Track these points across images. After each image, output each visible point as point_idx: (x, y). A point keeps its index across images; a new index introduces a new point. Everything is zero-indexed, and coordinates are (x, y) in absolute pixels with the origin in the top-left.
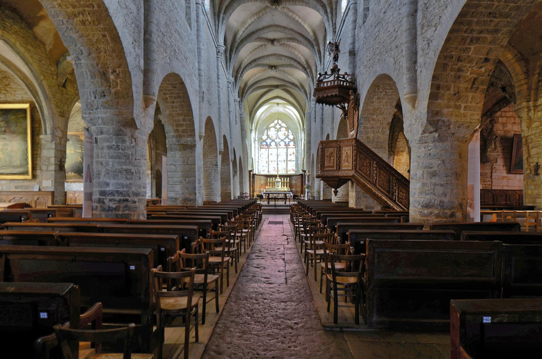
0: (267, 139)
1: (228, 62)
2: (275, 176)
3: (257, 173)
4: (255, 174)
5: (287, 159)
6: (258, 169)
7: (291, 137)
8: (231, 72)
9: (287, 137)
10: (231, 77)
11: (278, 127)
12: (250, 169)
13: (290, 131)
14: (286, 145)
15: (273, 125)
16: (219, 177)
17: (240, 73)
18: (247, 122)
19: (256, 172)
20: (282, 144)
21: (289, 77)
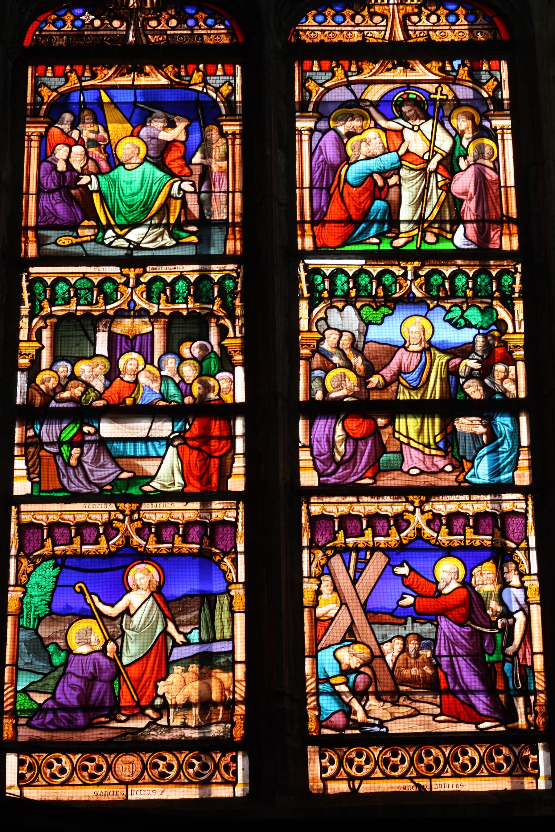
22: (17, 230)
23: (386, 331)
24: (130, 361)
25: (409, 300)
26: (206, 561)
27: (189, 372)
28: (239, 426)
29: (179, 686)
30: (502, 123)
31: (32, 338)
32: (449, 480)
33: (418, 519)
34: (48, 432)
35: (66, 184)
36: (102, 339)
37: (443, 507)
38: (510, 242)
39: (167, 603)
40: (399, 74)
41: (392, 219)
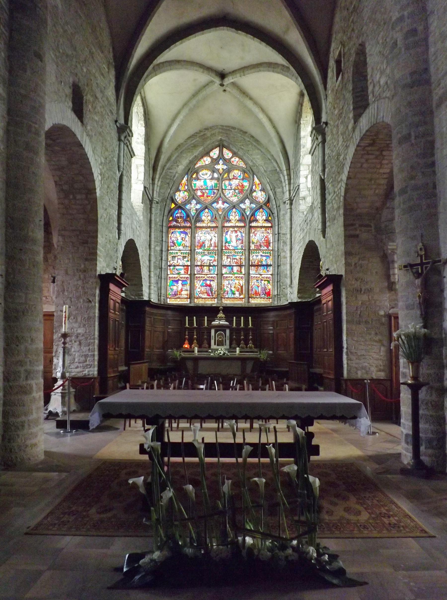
2: (212, 311)
3: (154, 299)
4: (148, 303)
6: (160, 289)
7: (260, 196)
11: (221, 166)
13: (256, 181)
15: (207, 160)
19: (149, 293)
20: (234, 216)
22: (168, 247)
23: (203, 258)
24: (179, 261)
25: (206, 255)
27: (185, 262)
28: (189, 267)
29: (183, 293)
32: (209, 273)
33: (206, 277)
34: (172, 268)
35: (173, 242)
36: (176, 258)
37: (208, 276)
38: (216, 249)
40: (206, 230)
41: (205, 246)
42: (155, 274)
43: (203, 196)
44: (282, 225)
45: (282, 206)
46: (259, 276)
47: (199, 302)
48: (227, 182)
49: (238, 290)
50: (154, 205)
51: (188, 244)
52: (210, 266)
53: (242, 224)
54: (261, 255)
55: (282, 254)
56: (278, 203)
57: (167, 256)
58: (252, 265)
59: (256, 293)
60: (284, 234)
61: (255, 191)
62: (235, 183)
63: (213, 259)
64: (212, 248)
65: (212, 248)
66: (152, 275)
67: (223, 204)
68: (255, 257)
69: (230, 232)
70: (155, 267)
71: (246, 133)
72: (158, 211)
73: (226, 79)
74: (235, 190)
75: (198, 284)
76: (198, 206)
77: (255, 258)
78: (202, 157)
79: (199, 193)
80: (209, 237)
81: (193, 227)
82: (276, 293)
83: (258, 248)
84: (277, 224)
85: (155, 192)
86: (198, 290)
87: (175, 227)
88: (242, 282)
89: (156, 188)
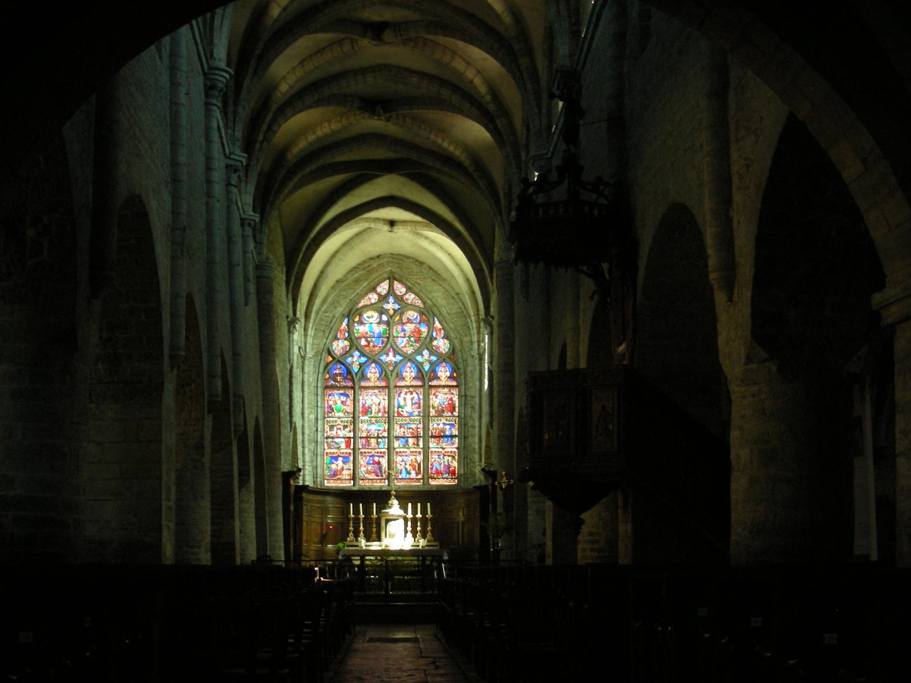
0: (347, 353)
1: (231, 102)
2: (382, 497)
3: (309, 482)
4: (305, 488)
5: (426, 429)
7: (442, 345)
8: (239, 134)
9: (427, 343)
10: (238, 151)
11: (391, 306)
12: (285, 467)
13: (438, 325)
14: (420, 375)
15: (373, 298)
16: (207, 488)
17: (265, 127)
18: (280, 292)
20: (409, 373)
21: (433, 137)
23: (369, 428)
26: (348, 457)
29: (344, 472)
30: (386, 398)
31: (327, 428)
34: (330, 440)
35: (330, 407)
39: (344, 462)
42: (309, 450)
43: (368, 346)
44: (470, 384)
45: (470, 360)
46: (440, 450)
47: (365, 485)
48: (399, 327)
49: (414, 469)
50: (307, 362)
51: (350, 410)
52: (378, 437)
53: (420, 383)
54: (444, 424)
55: (470, 423)
56: (465, 356)
57: (324, 425)
58: (432, 437)
59: (438, 472)
60: (472, 397)
61: (436, 339)
62: (409, 327)
63: (382, 429)
64: (380, 415)
65: (380, 415)
66: (306, 451)
67: (395, 356)
68: (435, 426)
69: (403, 395)
70: (309, 440)
71: (422, 263)
72: (312, 368)
73: (396, 228)
74: (409, 337)
75: (362, 461)
76: (363, 359)
77: (436, 425)
78: (367, 294)
79: (363, 342)
80: (376, 400)
81: (357, 387)
82: (462, 472)
83: (440, 413)
84: (463, 382)
85: (308, 346)
86: (363, 469)
87: (333, 387)
88: (420, 458)
89: (310, 340)
